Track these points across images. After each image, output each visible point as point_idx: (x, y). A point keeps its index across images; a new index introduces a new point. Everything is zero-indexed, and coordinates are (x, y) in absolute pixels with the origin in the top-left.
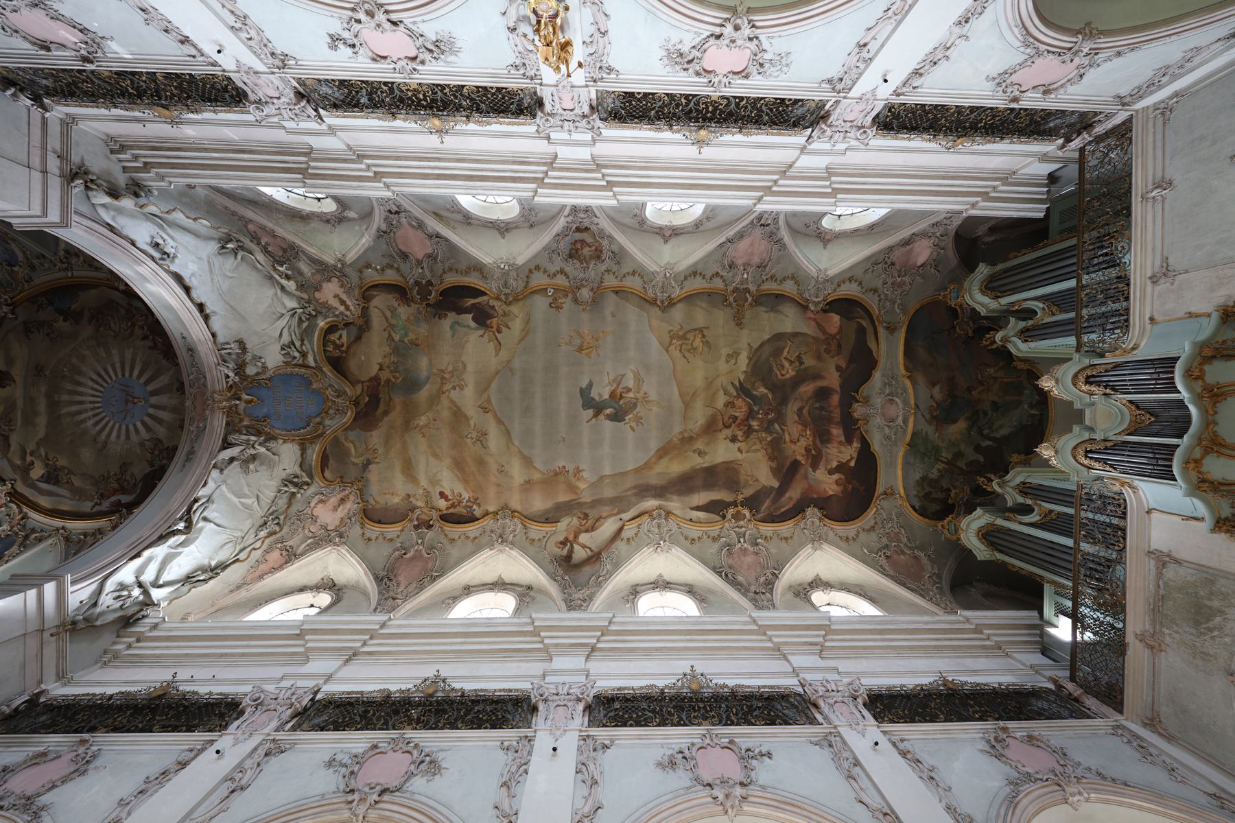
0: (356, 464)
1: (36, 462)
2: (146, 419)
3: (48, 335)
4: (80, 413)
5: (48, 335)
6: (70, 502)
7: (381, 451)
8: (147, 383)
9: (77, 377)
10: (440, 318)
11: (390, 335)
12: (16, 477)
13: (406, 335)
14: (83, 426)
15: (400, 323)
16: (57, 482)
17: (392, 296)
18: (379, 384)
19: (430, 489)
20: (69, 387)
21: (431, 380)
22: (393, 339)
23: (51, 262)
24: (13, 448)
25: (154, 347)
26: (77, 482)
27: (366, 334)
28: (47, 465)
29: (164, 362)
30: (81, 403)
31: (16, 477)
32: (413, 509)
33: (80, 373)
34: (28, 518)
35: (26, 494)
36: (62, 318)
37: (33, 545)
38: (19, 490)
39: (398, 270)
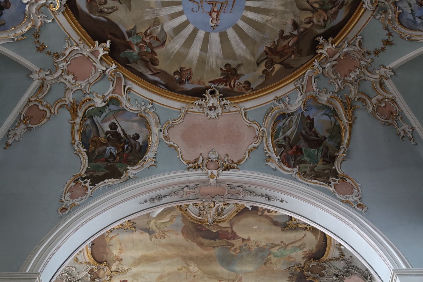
0: (149, 224)
2: (190, 28)
7: (163, 241)
8: (237, 29)
10: (289, 277)
11: (276, 245)
13: (276, 256)
15: (287, 253)
17: (314, 247)
18: (229, 239)
19: (128, 274)
21: (231, 272)
22: (272, 248)
25: (282, 36)
27: (279, 229)
29: (262, 49)
32: (109, 265)
39: (337, 259)
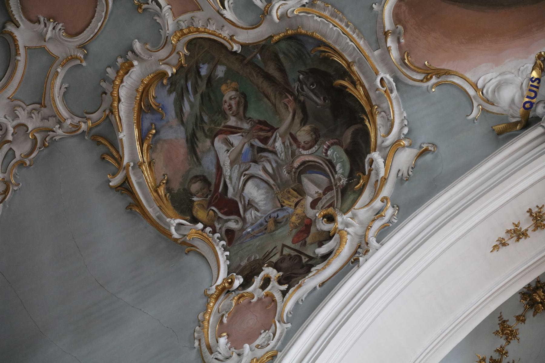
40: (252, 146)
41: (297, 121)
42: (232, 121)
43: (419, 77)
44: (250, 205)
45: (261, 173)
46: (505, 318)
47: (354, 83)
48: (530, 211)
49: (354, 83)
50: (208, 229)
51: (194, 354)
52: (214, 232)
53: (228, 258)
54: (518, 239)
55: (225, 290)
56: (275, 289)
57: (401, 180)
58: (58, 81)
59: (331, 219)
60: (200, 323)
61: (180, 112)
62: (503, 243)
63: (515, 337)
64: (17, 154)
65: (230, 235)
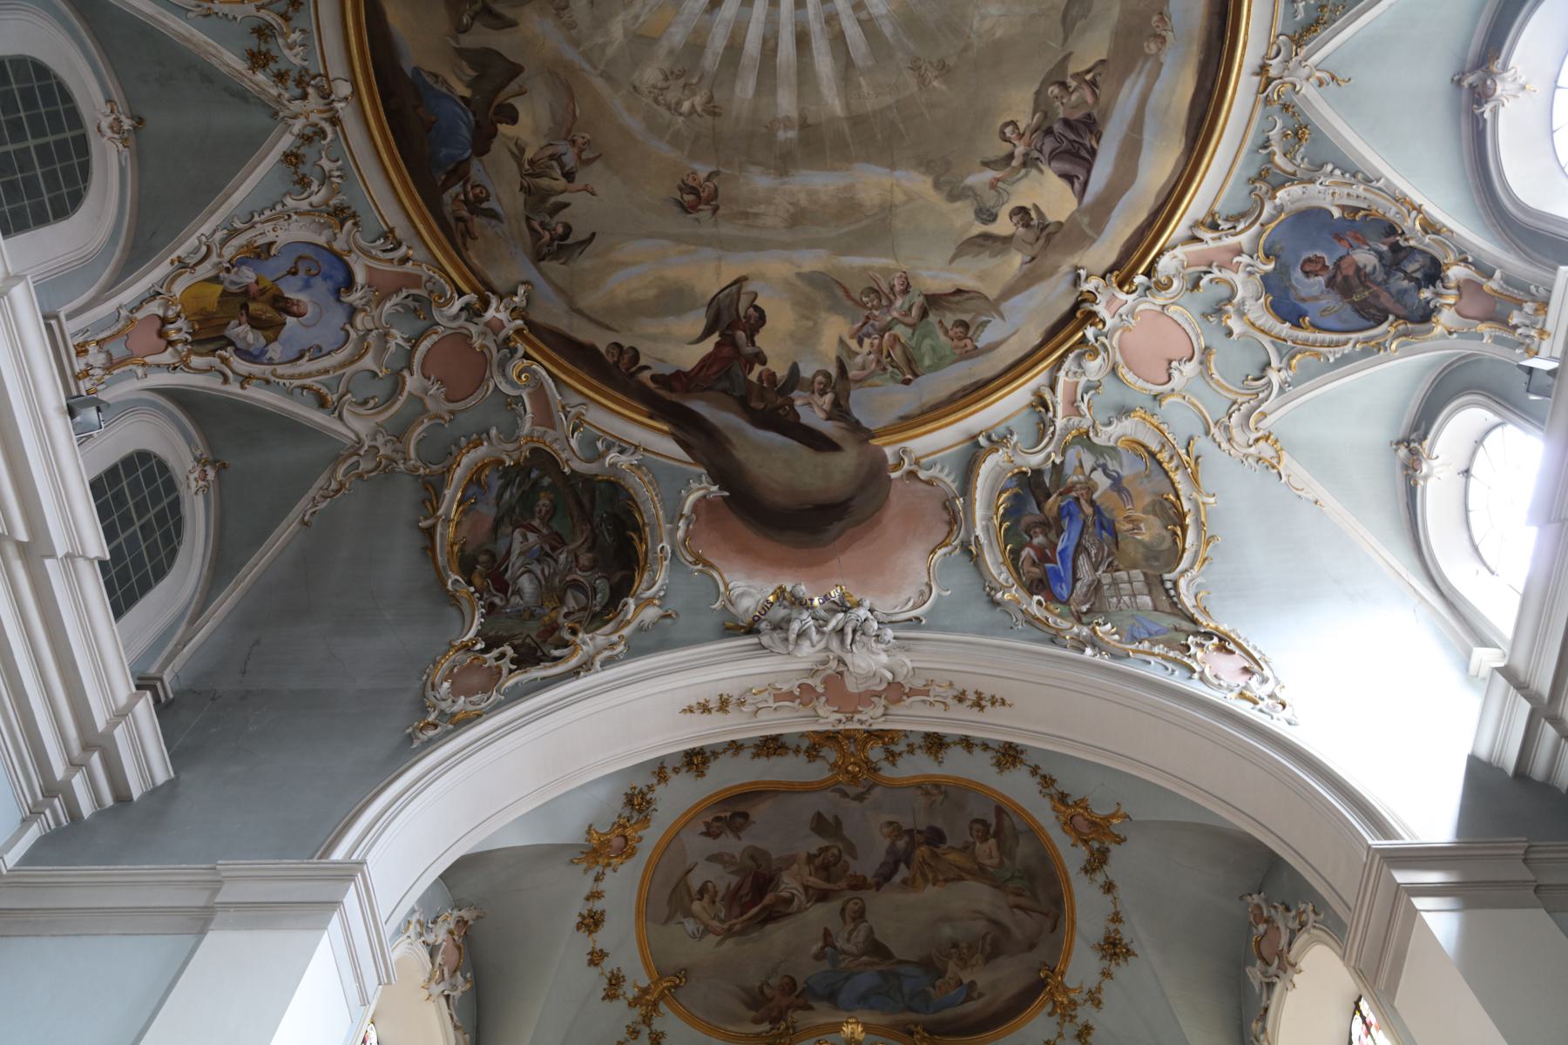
1: (1015, 202)
3: (569, 176)
4: (838, 40)
5: (569, 176)
6: (1164, 70)
9: (710, 61)
12: (1066, 268)
14: (887, 30)
16: (1090, 125)
20: (746, 87)
23: (306, 139)
24: (968, 282)
26: (1092, 48)
28: (1028, 162)
30: (802, 40)
31: (1066, 268)
33: (695, 47)
34: (1212, 214)
35: (1128, 232)
36: (503, 128)
37: (1320, 138)
38: (1111, 258)
40: (542, 548)
41: (585, 546)
42: (536, 523)
43: (690, 559)
44: (518, 592)
45: (539, 572)
46: (665, 765)
47: (641, 540)
48: (721, 696)
49: (641, 540)
50: (477, 595)
51: (418, 685)
52: (480, 599)
53: (481, 624)
54: (704, 712)
55: (467, 648)
56: (506, 665)
57: (641, 629)
58: (421, 429)
59: (574, 632)
60: (435, 663)
61: (500, 497)
62: (691, 710)
63: (666, 781)
64: (361, 467)
65: (491, 608)
